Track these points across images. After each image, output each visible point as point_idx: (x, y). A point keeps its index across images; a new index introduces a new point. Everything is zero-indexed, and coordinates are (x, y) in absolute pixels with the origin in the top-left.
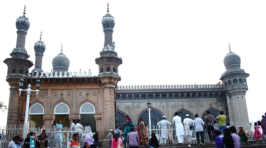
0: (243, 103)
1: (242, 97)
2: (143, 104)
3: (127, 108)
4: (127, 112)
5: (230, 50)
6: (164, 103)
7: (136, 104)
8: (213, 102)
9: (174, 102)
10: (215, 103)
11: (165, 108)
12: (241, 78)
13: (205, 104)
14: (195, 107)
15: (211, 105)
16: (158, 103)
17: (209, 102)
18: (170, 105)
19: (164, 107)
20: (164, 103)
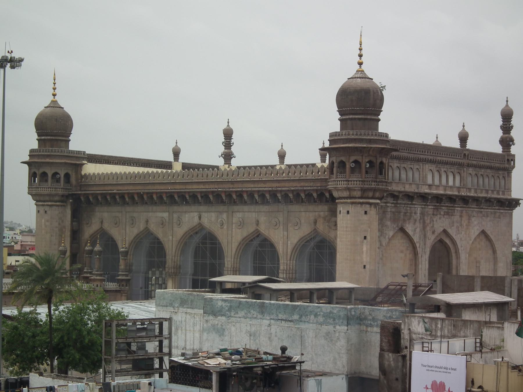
0: (347, 227)
1: (348, 212)
2: (187, 216)
3: (161, 226)
4: (160, 234)
5: (360, 64)
6: (225, 216)
7: (175, 216)
8: (320, 216)
9: (239, 215)
10: (324, 218)
11: (225, 227)
12: (343, 159)
13: (303, 221)
14: (281, 227)
15: (315, 222)
16: (213, 214)
17: (312, 216)
18: (234, 221)
19: (222, 225)
20: (225, 216)
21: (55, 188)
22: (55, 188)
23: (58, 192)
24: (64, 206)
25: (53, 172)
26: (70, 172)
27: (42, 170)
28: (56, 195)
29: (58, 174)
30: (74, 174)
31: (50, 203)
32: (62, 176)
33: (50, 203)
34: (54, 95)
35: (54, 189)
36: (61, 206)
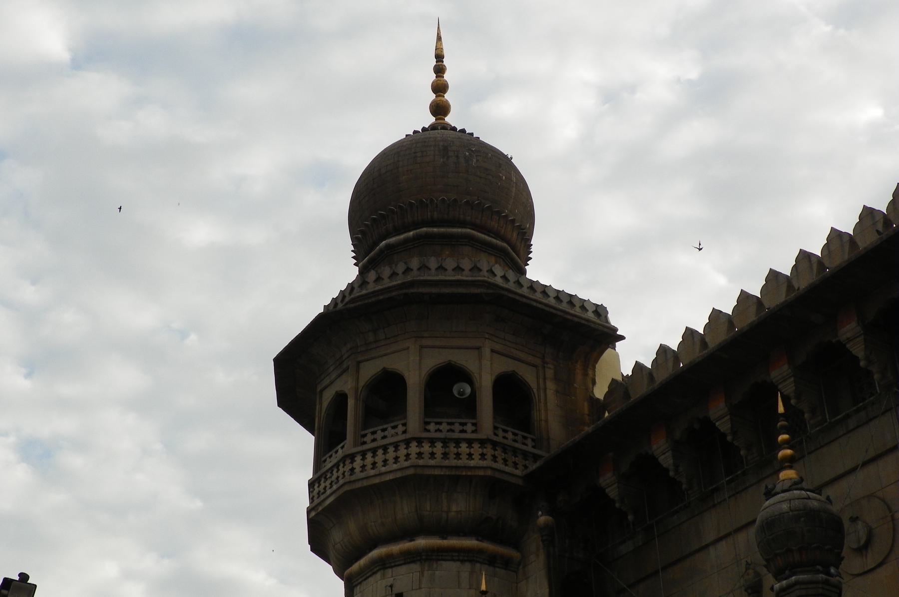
21: (445, 442)
22: (445, 442)
23: (464, 461)
24: (507, 563)
25: (434, 360)
26: (529, 376)
27: (370, 370)
28: (455, 481)
29: (463, 375)
30: (551, 386)
31: (422, 542)
32: (486, 382)
33: (422, 542)
34: (440, 109)
35: (439, 448)
36: (492, 560)
